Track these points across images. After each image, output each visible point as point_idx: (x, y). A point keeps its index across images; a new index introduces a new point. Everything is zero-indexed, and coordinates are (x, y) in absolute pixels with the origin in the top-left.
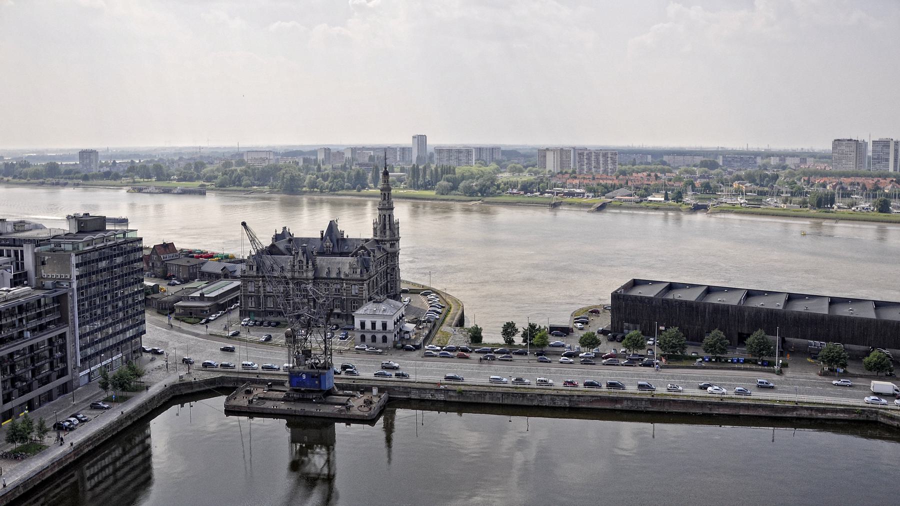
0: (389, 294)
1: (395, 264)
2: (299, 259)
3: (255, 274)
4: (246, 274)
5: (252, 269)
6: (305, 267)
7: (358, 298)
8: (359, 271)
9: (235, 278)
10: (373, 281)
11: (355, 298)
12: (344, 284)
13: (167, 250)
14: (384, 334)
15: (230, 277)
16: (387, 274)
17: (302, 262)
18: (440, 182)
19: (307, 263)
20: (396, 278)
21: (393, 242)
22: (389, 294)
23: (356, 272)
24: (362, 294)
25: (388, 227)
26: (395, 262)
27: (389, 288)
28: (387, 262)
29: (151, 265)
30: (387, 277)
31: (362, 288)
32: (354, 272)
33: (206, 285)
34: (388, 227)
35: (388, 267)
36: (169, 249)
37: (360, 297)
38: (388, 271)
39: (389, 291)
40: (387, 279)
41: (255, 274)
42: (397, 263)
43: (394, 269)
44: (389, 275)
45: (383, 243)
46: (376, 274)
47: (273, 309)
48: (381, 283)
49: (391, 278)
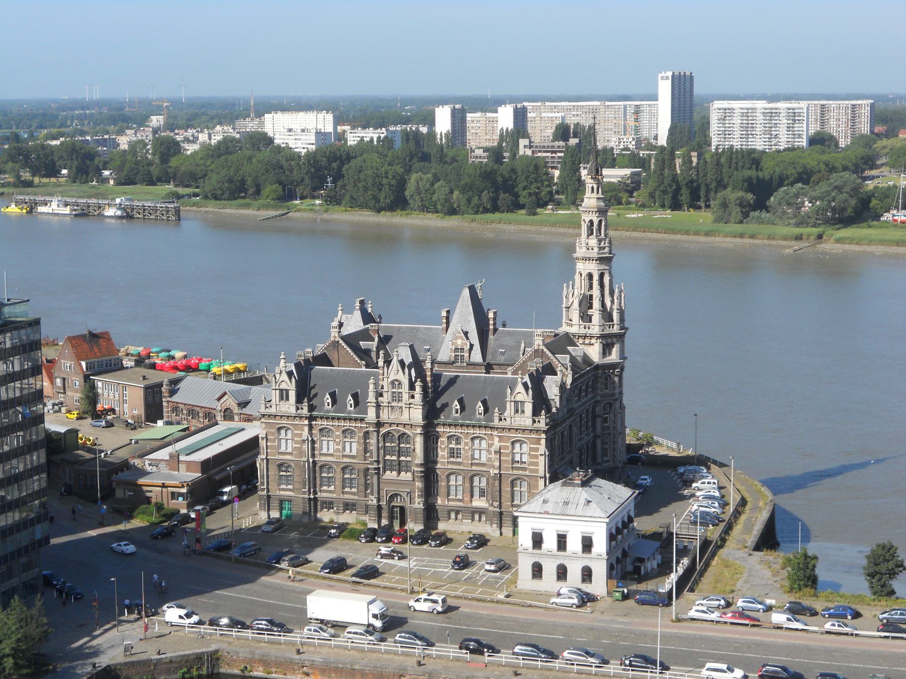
0: (599, 467)
1: (614, 395)
2: (392, 378)
3: (292, 410)
4: (273, 410)
5: (287, 399)
6: (405, 397)
7: (527, 473)
8: (529, 408)
9: (249, 419)
10: (562, 433)
11: (521, 472)
12: (496, 439)
13: (96, 350)
14: (586, 563)
15: (236, 418)
16: (595, 417)
17: (400, 383)
18: (723, 192)
19: (412, 387)
20: (614, 428)
21: (609, 341)
22: (599, 467)
23: (523, 412)
24: (537, 464)
25: (596, 304)
26: (614, 388)
27: (599, 451)
28: (594, 389)
29: (59, 382)
30: (594, 425)
31: (537, 450)
32: (517, 411)
33: (183, 433)
34: (596, 304)
35: (597, 402)
36: (99, 345)
37: (532, 471)
38: (598, 410)
39: (599, 460)
40: (594, 430)
41: (292, 410)
42: (617, 391)
43: (611, 405)
44: (599, 421)
45: (587, 341)
46: (568, 418)
47: (334, 495)
48: (580, 440)
49: (603, 429)
